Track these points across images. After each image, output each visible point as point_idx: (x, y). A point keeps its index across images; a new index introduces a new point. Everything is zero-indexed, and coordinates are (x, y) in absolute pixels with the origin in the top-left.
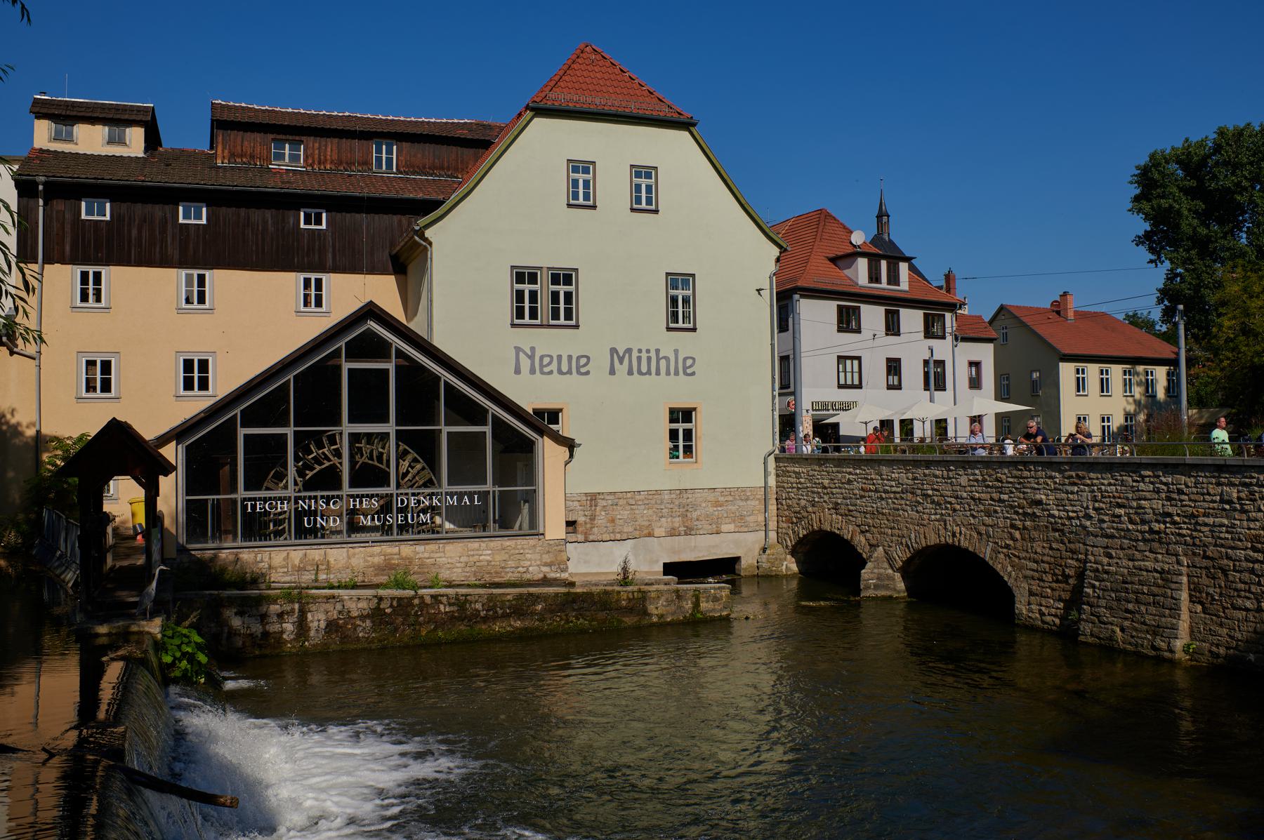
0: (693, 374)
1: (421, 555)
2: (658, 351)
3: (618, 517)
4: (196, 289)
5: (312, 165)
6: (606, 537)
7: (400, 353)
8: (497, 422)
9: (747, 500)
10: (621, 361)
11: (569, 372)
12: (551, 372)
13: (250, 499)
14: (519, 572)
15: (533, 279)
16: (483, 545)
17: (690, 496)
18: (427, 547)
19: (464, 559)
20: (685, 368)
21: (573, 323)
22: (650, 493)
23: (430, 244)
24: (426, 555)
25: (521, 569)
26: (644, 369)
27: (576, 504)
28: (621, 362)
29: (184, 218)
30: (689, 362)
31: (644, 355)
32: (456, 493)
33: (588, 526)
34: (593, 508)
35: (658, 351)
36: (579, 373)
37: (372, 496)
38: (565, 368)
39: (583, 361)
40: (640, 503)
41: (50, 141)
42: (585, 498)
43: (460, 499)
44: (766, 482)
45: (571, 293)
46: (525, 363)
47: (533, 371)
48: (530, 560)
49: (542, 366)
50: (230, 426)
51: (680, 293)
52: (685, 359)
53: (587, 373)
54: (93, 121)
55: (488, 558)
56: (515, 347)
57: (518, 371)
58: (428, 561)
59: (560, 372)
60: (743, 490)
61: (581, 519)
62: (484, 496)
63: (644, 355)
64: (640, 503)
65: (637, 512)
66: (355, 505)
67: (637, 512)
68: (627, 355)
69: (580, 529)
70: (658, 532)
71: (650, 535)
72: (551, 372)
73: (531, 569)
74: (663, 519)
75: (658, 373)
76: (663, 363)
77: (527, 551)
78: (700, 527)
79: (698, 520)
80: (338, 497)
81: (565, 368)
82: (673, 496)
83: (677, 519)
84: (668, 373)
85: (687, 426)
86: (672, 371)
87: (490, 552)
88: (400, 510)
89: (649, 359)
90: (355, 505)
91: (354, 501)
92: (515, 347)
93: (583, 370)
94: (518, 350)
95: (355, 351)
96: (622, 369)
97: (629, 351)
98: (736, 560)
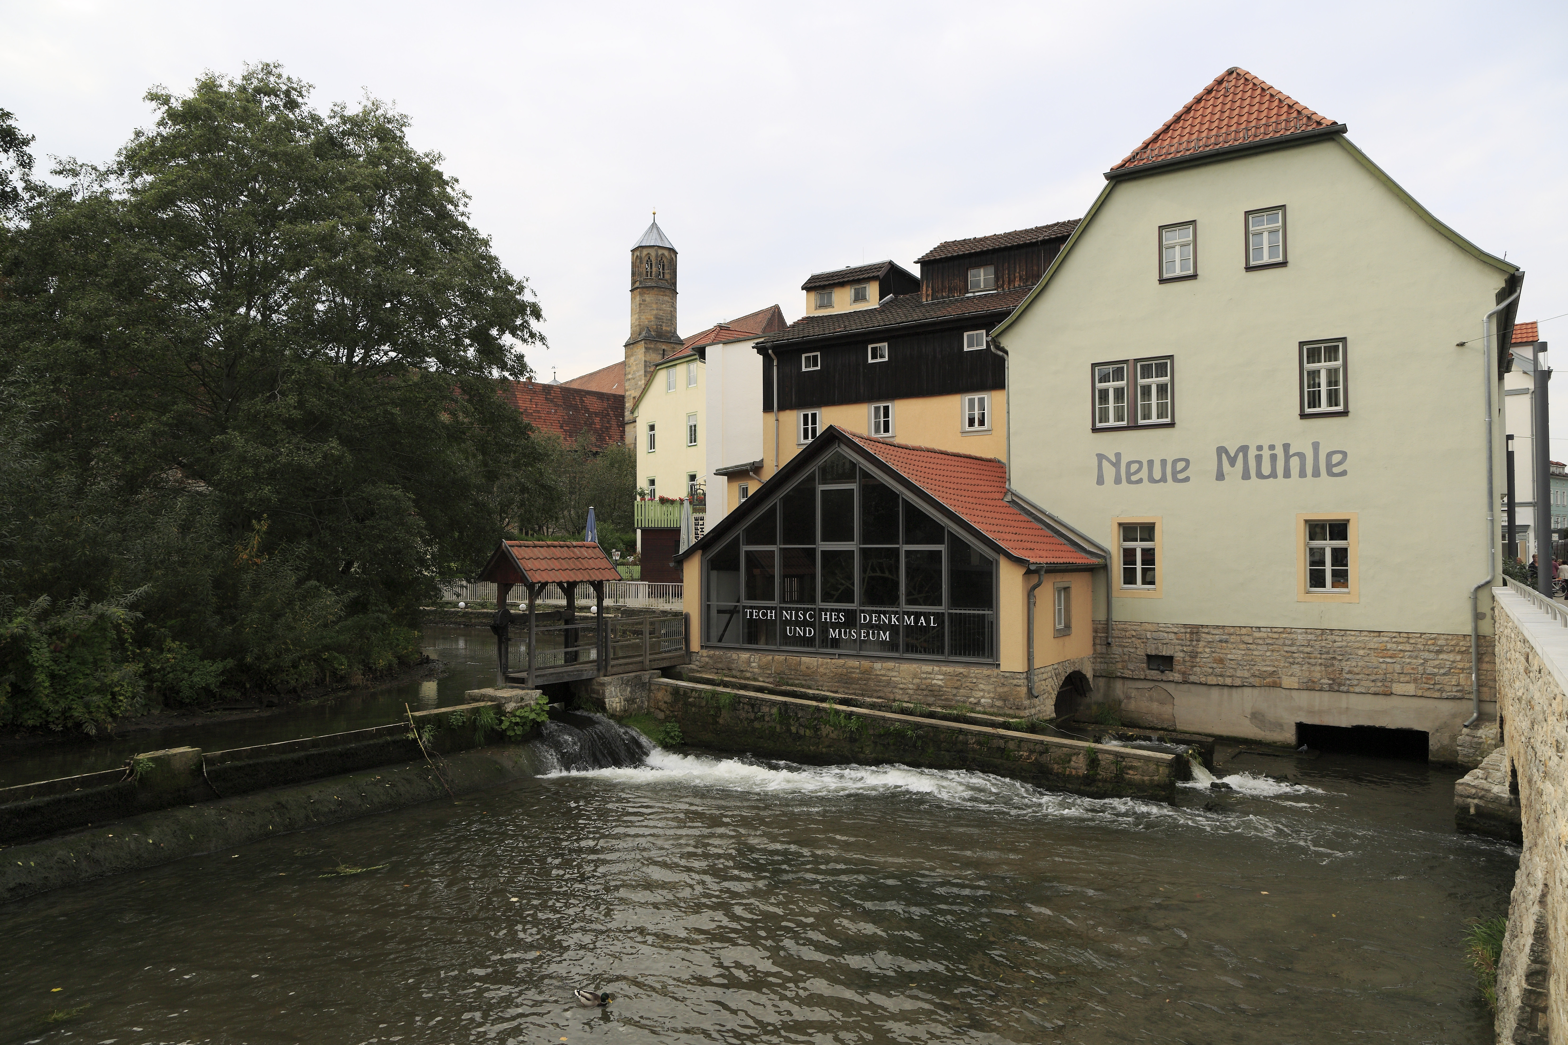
0: (1344, 473)
1: (878, 673)
2: (1286, 447)
3: (1229, 656)
4: (882, 420)
5: (1002, 286)
6: (1212, 680)
7: (866, 475)
8: (954, 539)
9: (1439, 652)
10: (1232, 462)
11: (1163, 479)
12: (1140, 481)
13: (752, 608)
14: (970, 703)
15: (1118, 374)
16: (936, 669)
17: (1337, 638)
18: (884, 665)
19: (916, 681)
20: (1329, 466)
21: (1340, 408)
22: (1276, 630)
23: (1006, 353)
24: (883, 672)
25: (972, 700)
26: (1266, 470)
27: (1172, 636)
28: (1232, 462)
29: (872, 358)
30: (1336, 458)
31: (1266, 454)
32: (913, 613)
33: (1188, 664)
34: (1194, 643)
35: (1286, 447)
36: (1175, 480)
37: (839, 611)
38: (1157, 475)
39: (1180, 465)
40: (1261, 642)
41: (816, 309)
42: (1183, 630)
43: (917, 620)
44: (1476, 628)
45: (1123, 389)
46: (1109, 472)
47: (1118, 481)
48: (983, 690)
49: (1129, 475)
50: (735, 543)
51: (1323, 366)
52: (1329, 455)
53: (1187, 479)
54: (842, 284)
55: (940, 683)
56: (1098, 455)
57: (1100, 481)
58: (884, 678)
59: (1152, 480)
60: (1436, 637)
61: (1179, 656)
62: (939, 617)
63: (1266, 454)
64: (1261, 642)
65: (1255, 653)
66: (826, 619)
67: (1255, 653)
68: (1241, 455)
69: (1177, 667)
70: (1286, 682)
71: (1276, 685)
72: (1140, 481)
73: (983, 701)
74: (1295, 666)
75: (1287, 474)
76: (1295, 462)
77: (980, 681)
78: (1355, 682)
79: (1350, 672)
80: (811, 609)
81: (1157, 475)
82: (1310, 637)
83: (1318, 668)
84: (1303, 474)
85: (1147, 545)
86: (1309, 470)
87: (941, 677)
88: (862, 626)
89: (1274, 458)
90: (826, 619)
91: (826, 614)
92: (1098, 455)
93: (1180, 476)
94: (1101, 457)
95: (827, 474)
96: (1234, 473)
97: (1244, 449)
98: (1421, 738)
